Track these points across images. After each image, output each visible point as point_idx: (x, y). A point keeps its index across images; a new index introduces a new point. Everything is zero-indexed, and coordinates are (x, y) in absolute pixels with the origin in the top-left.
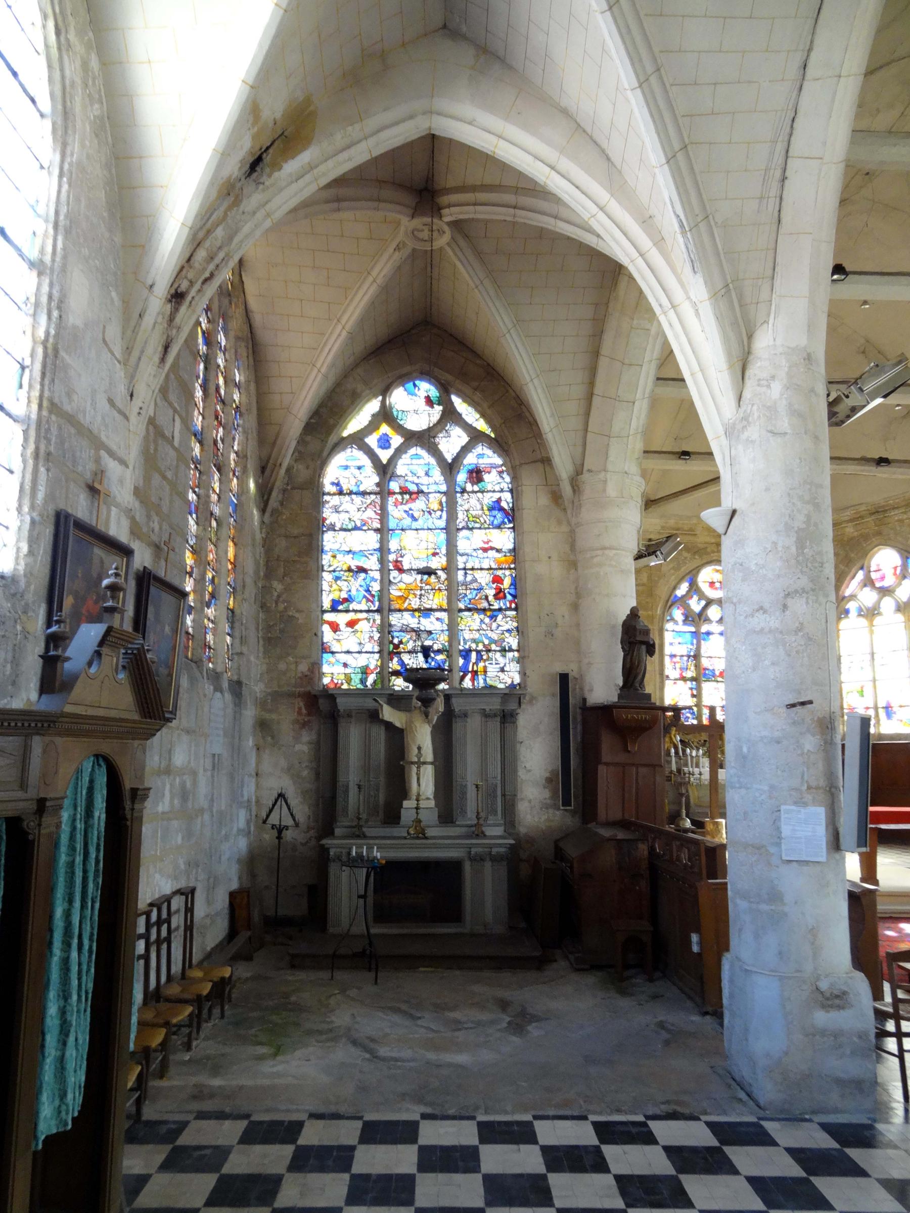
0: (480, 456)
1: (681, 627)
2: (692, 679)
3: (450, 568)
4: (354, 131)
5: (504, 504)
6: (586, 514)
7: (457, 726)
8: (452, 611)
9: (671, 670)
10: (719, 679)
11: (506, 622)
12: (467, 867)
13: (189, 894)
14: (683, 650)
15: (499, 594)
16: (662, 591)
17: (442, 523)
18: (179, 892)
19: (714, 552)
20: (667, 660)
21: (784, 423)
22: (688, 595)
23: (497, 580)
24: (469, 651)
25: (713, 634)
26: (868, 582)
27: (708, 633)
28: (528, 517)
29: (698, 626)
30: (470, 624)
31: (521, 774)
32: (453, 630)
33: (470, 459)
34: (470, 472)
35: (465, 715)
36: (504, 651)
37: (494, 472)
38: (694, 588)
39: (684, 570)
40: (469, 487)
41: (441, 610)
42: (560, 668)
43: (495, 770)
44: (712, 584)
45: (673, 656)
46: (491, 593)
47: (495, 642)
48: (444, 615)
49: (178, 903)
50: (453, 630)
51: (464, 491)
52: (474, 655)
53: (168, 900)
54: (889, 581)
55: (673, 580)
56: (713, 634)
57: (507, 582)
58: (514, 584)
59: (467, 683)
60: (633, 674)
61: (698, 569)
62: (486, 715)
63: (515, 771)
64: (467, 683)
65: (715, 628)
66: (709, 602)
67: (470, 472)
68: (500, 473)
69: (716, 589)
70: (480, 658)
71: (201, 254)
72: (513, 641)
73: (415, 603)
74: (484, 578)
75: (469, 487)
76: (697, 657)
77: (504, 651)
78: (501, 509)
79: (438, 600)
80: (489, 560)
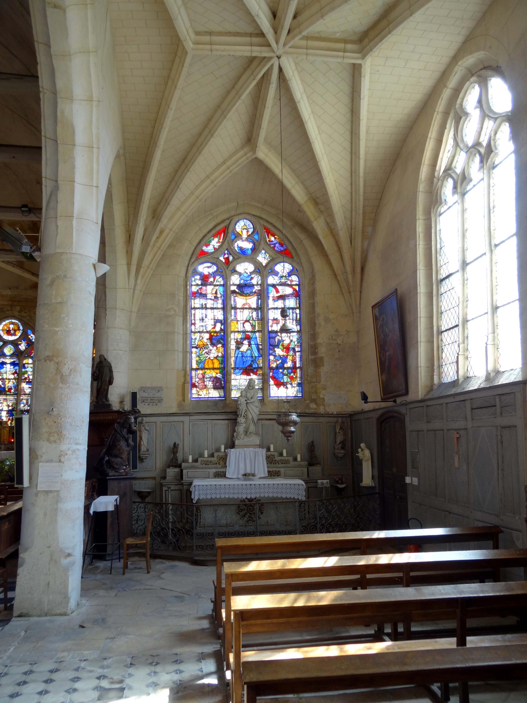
10: (8, 393)
19: (8, 311)
25: (5, 363)
44: (8, 332)
56: (5, 363)
65: (8, 360)
69: (12, 335)
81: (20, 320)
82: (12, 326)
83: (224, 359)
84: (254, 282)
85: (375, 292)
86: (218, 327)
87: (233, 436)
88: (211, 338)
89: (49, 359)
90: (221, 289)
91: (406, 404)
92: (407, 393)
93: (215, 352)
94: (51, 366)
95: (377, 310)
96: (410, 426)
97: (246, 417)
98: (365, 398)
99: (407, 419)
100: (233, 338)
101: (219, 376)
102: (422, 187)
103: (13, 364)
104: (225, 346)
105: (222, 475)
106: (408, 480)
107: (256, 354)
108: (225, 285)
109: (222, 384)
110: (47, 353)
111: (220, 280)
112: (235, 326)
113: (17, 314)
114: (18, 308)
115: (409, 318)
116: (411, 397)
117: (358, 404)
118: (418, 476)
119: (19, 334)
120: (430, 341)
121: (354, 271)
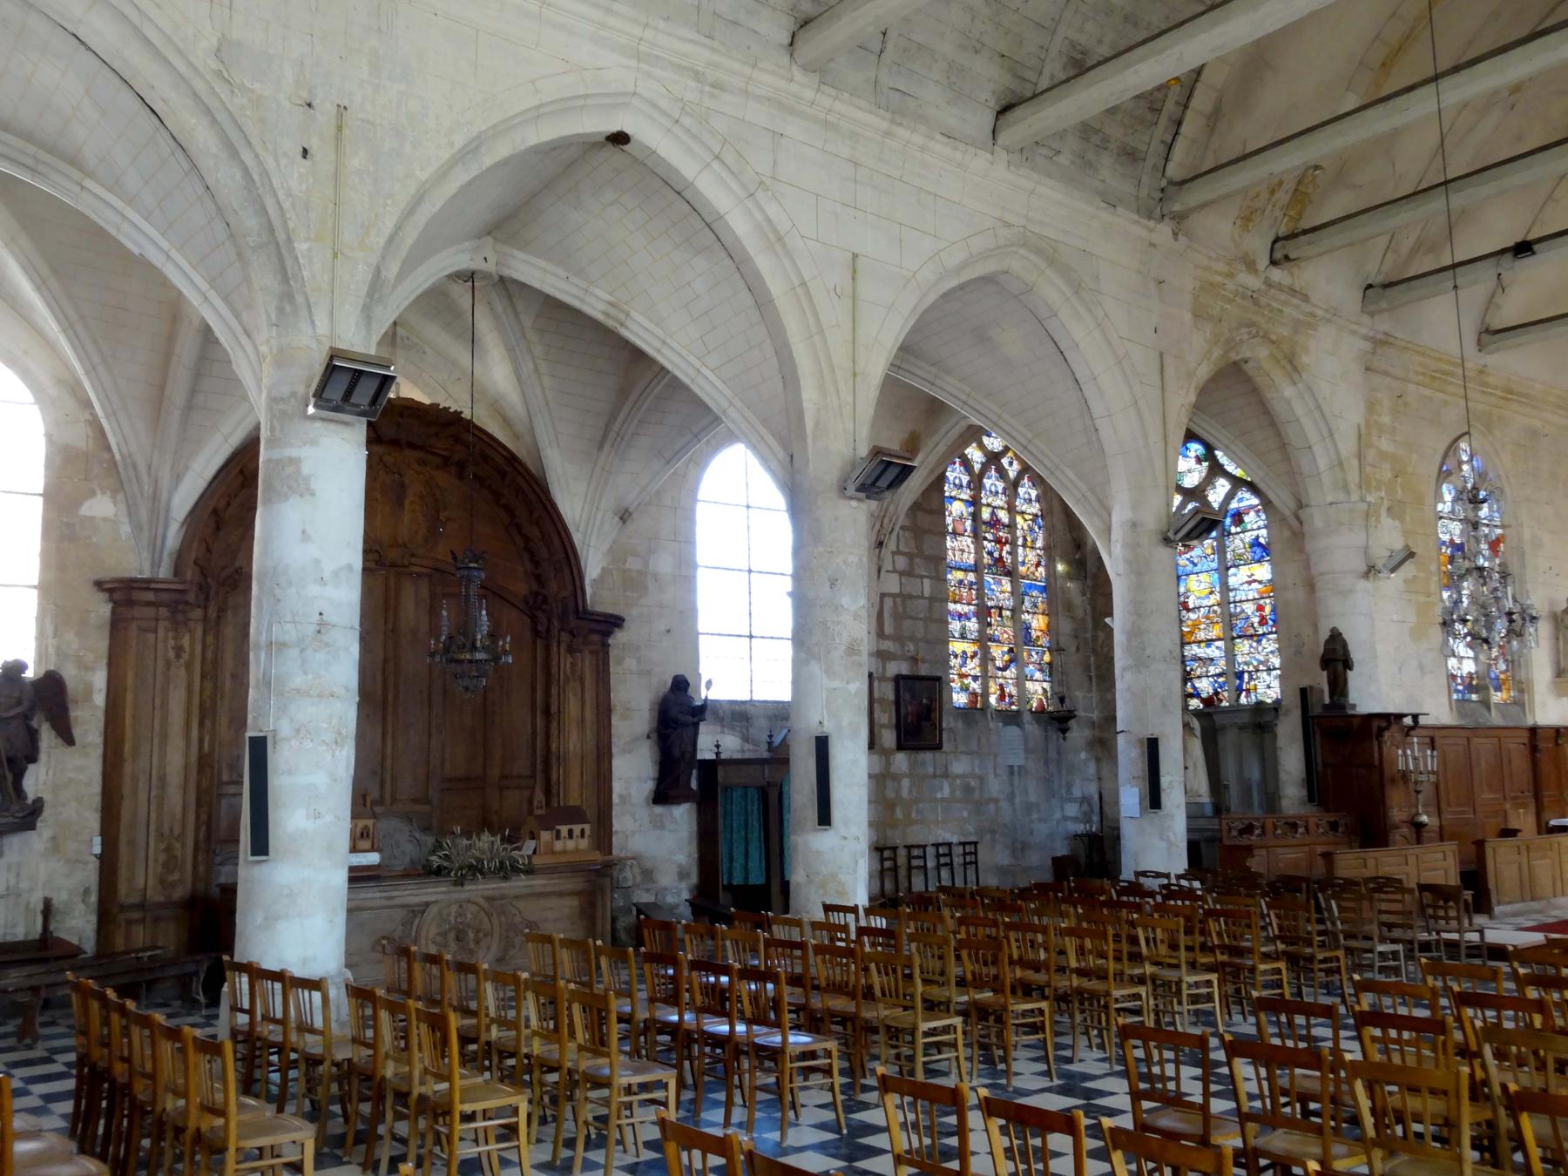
0: (1241, 500)
3: (1224, 603)
4: (936, 438)
5: (1262, 540)
6: (1309, 546)
7: (1221, 740)
8: (1230, 640)
11: (1269, 645)
12: (1203, 845)
13: (970, 849)
15: (1263, 622)
17: (1215, 565)
18: (964, 844)
23: (1260, 608)
24: (1243, 672)
28: (1274, 549)
30: (1243, 647)
31: (1283, 776)
32: (1230, 655)
33: (1234, 505)
34: (1233, 516)
35: (1223, 728)
36: (1269, 670)
37: (1252, 513)
40: (1233, 530)
41: (1219, 639)
42: (1305, 683)
43: (1254, 773)
46: (1256, 620)
47: (1260, 662)
50: (1230, 655)
51: (1230, 534)
52: (1246, 676)
53: (949, 845)
57: (1268, 609)
58: (1273, 611)
59: (1243, 700)
60: (1338, 686)
62: (1242, 728)
63: (1276, 774)
67: (1233, 516)
68: (1257, 512)
70: (1251, 678)
71: (886, 520)
72: (1276, 661)
73: (1201, 635)
74: (1249, 608)
75: (1233, 530)
77: (1269, 670)
78: (1260, 545)
79: (1216, 631)
80: (1252, 592)
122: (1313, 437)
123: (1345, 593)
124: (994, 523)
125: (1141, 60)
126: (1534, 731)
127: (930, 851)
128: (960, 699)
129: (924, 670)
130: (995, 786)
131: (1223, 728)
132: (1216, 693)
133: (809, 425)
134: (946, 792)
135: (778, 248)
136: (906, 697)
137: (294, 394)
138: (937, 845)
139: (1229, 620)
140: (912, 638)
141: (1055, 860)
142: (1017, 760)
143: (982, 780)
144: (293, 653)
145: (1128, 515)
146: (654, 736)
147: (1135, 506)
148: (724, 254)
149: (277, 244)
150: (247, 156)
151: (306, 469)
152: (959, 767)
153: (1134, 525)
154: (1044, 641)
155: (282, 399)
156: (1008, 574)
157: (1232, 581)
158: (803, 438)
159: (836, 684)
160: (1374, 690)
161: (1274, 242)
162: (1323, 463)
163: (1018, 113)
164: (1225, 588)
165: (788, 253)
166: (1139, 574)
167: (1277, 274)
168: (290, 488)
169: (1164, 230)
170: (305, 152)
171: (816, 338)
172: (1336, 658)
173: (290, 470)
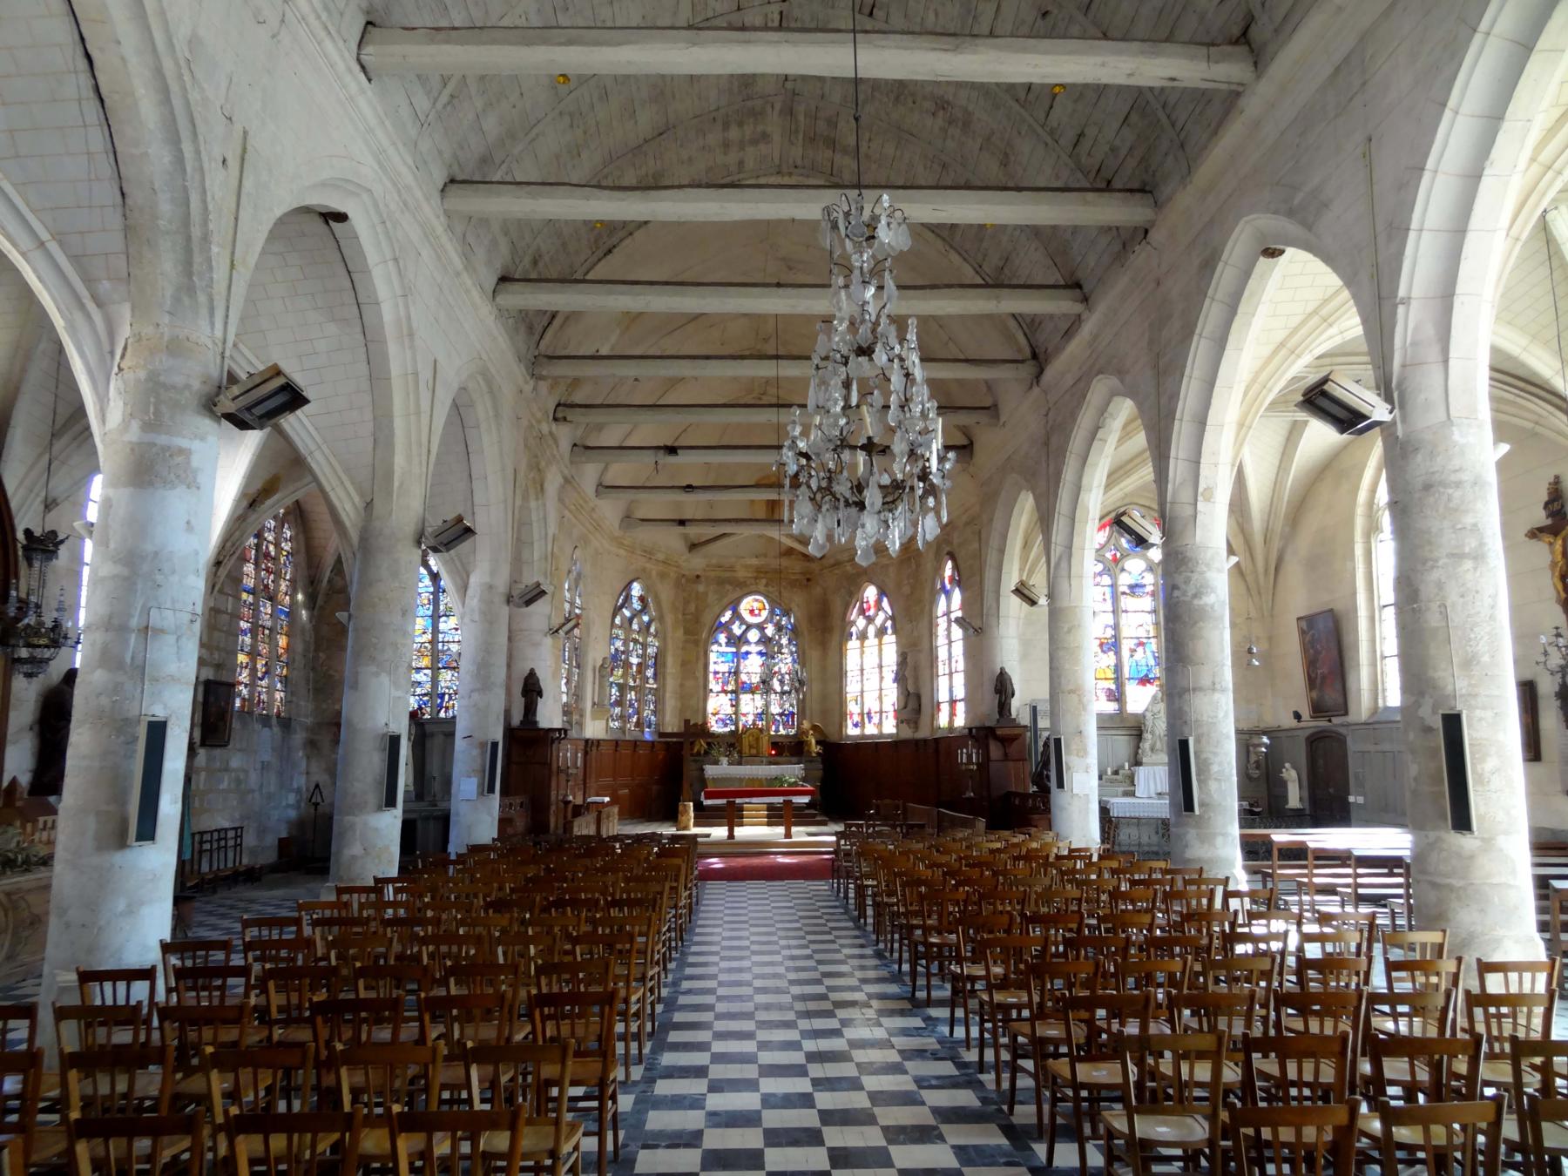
1: (724, 649)
2: (732, 692)
3: (434, 642)
7: (428, 745)
8: (435, 670)
9: (714, 685)
12: (419, 825)
13: (238, 831)
14: (724, 668)
16: (707, 618)
18: (235, 829)
20: (711, 676)
21: (477, 618)
22: (731, 621)
26: (862, 612)
27: (748, 653)
29: (738, 648)
32: (435, 681)
35: (432, 735)
38: (737, 616)
39: (726, 601)
44: (752, 612)
45: (716, 673)
48: (428, 672)
49: (231, 834)
50: (435, 681)
53: (226, 830)
54: (871, 613)
55: (717, 610)
59: (442, 714)
60: (530, 709)
61: (738, 601)
64: (442, 714)
65: (754, 649)
66: (749, 627)
76: (737, 673)
79: (426, 662)
81: (766, 597)
82: (756, 605)
83: (1118, 668)
84: (1144, 582)
85: (1297, 600)
86: (1110, 632)
87: (1136, 753)
88: (1101, 645)
89: (1071, 692)
90: (1108, 590)
91: (1348, 725)
92: (1346, 713)
93: (1110, 659)
94: (1074, 697)
95: (1304, 624)
96: (1353, 746)
97: (1153, 733)
98: (1297, 716)
99: (1349, 740)
100: (1126, 646)
101: (1113, 687)
102: (1360, 510)
103: (760, 654)
104: (1118, 654)
105: (1132, 794)
106: (1351, 799)
107: (1152, 662)
108: (1113, 586)
109: (1117, 696)
110: (1070, 687)
111: (1106, 580)
112: (1126, 631)
113: (762, 588)
114: (764, 581)
115: (1347, 640)
116: (1351, 718)
117: (1288, 722)
118: (1364, 795)
119: (765, 614)
120: (1373, 664)
121: (1266, 570)
122: (536, 536)
123: (536, 645)
124: (267, 555)
125: (622, 293)
126: (587, 741)
127: (216, 836)
128: (238, 703)
129: (225, 678)
130: (253, 779)
131: (432, 735)
132: (420, 708)
133: (396, 484)
134: (224, 786)
135: (406, 340)
136: (212, 699)
137: (187, 386)
138: (219, 831)
139: (435, 655)
140: (218, 648)
141: (280, 840)
142: (266, 758)
143: (246, 772)
144: (171, 639)
145: (487, 579)
146: (36, 728)
147: (493, 573)
148: (359, 329)
149: (189, 239)
150: (187, 147)
151: (195, 461)
152: (236, 762)
153: (491, 587)
154: (284, 658)
155: (174, 387)
156: (271, 599)
157: (442, 626)
158: (390, 494)
159: (399, 693)
160: (549, 715)
161: (559, 405)
162: (536, 555)
163: (507, 284)
164: (436, 631)
165: (412, 347)
166: (491, 623)
167: (554, 426)
168: (178, 477)
169: (532, 383)
170: (224, 161)
171: (413, 418)
172: (532, 689)
173: (179, 459)
